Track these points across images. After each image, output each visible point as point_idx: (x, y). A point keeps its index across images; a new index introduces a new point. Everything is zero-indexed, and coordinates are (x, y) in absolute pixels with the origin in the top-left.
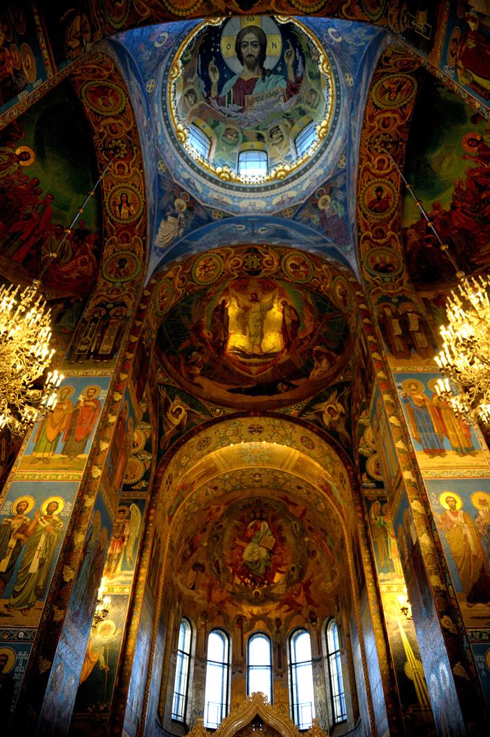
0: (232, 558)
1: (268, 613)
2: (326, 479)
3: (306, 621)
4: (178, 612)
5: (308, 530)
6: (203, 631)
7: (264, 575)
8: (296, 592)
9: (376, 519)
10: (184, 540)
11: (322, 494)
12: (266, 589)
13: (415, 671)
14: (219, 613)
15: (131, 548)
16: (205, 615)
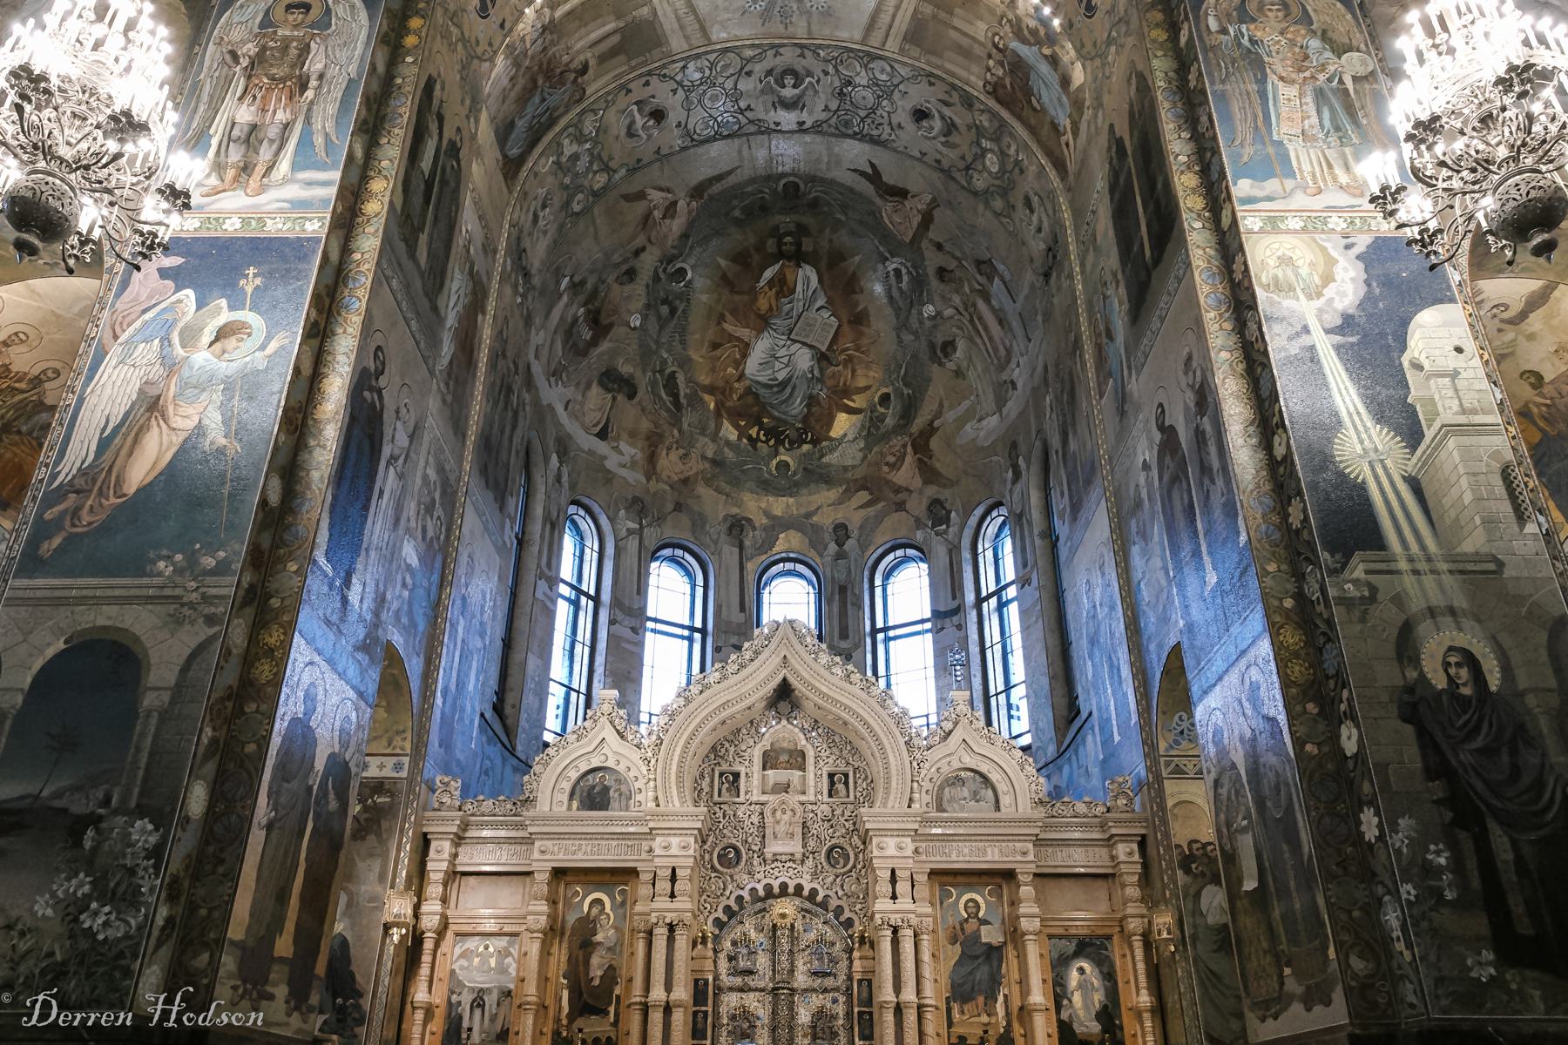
0: (713, 370)
1: (815, 512)
2: (1015, 45)
3: (919, 524)
4: (558, 479)
5: (934, 283)
6: (633, 544)
7: (805, 420)
8: (892, 459)
9: (1224, 31)
10: (565, 282)
11: (994, 115)
12: (808, 455)
13: (1373, 456)
14: (678, 507)
15: (332, 109)
16: (639, 507)
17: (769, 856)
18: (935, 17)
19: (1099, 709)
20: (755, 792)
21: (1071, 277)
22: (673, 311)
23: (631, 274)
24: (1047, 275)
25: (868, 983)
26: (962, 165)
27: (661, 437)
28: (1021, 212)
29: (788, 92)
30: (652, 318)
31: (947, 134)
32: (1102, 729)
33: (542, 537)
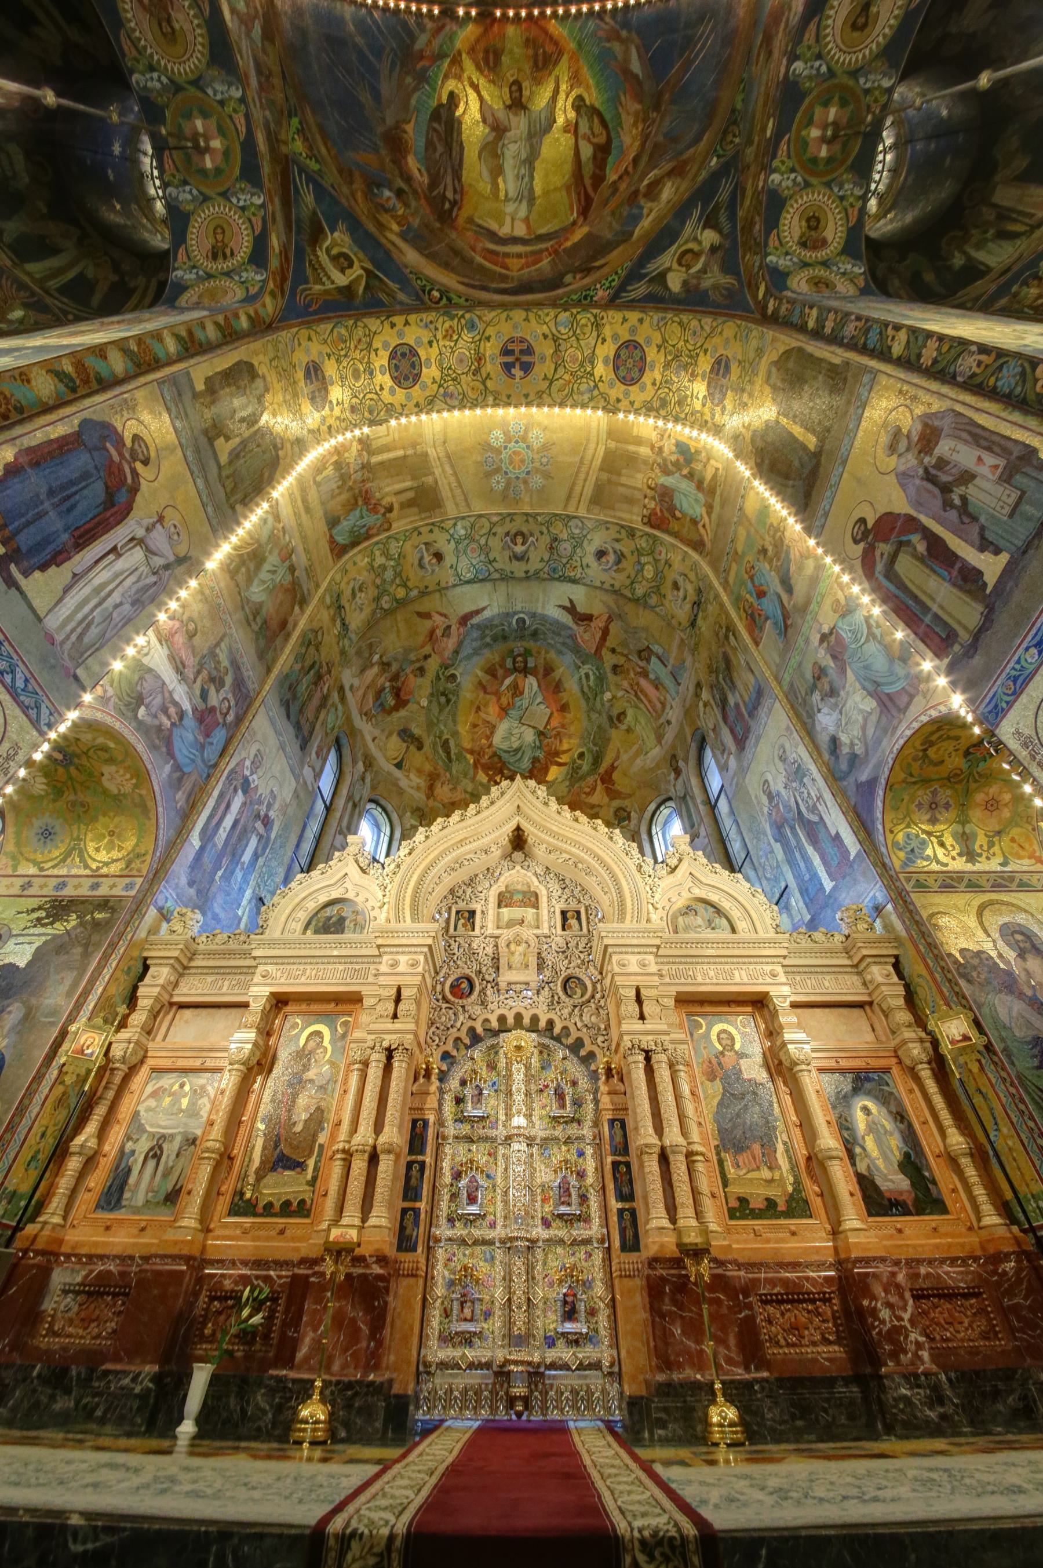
4: (363, 779)
10: (376, 658)
17: (503, 985)
18: (609, 481)
19: (798, 877)
20: (490, 925)
21: (717, 596)
22: (448, 701)
23: (421, 671)
24: (693, 624)
25: (619, 1123)
26: (628, 582)
27: (438, 776)
28: (670, 594)
29: (519, 549)
30: (435, 704)
31: (618, 562)
32: (804, 892)
33: (345, 809)
